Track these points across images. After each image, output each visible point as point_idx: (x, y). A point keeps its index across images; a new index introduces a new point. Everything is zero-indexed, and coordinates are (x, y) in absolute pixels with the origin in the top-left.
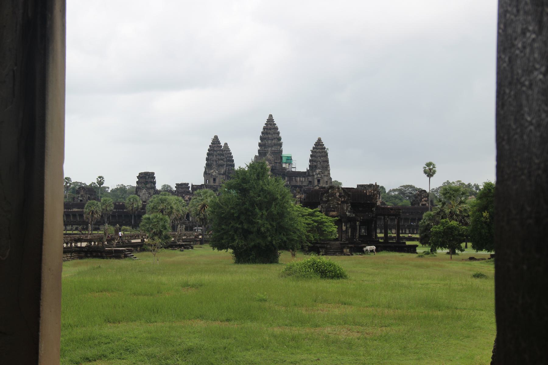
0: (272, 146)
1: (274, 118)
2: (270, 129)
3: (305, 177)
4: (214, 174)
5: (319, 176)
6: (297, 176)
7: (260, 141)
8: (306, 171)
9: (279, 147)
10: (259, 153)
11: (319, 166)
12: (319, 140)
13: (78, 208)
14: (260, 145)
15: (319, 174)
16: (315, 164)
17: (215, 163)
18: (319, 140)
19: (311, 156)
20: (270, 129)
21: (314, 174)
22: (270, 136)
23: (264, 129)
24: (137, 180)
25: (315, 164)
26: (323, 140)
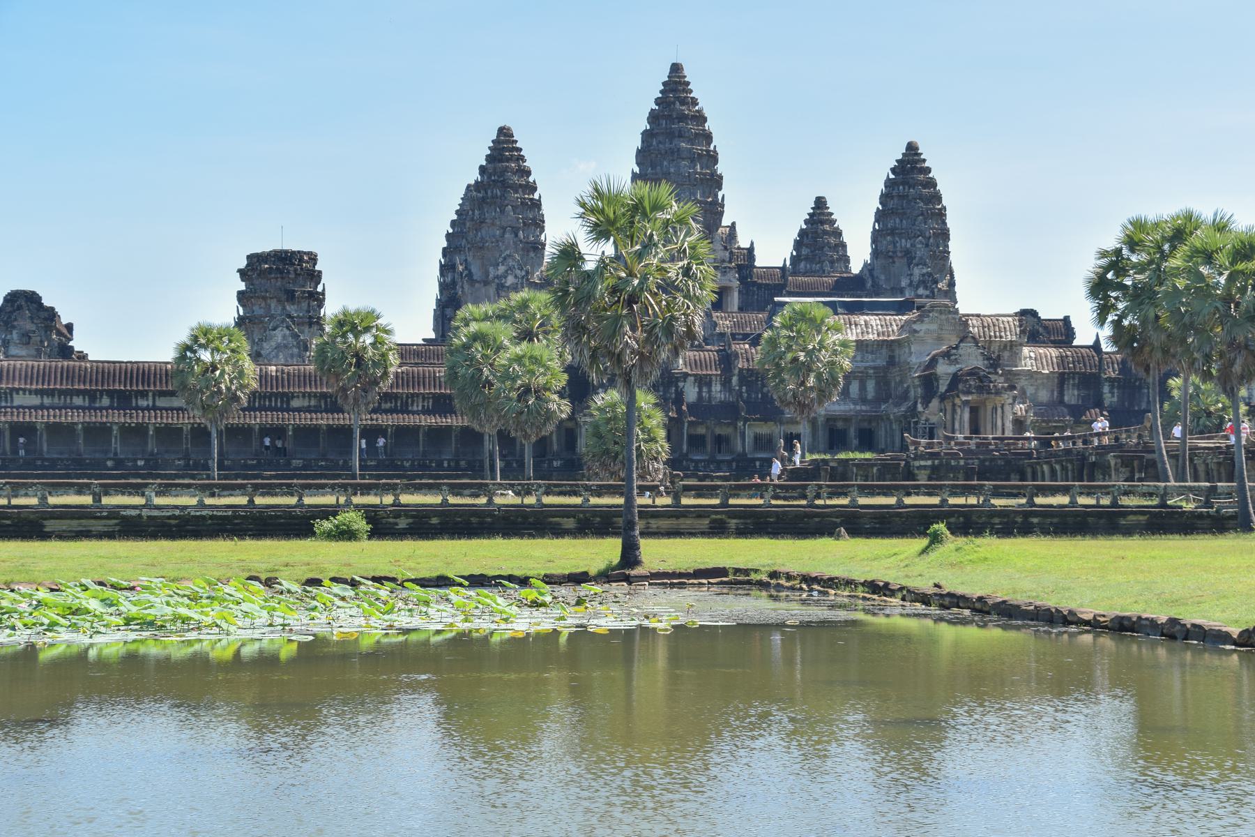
2: (683, 118)
4: (510, 280)
5: (921, 291)
12: (912, 148)
16: (905, 243)
18: (912, 148)
23: (653, 117)
24: (242, 286)
25: (905, 243)
26: (925, 151)
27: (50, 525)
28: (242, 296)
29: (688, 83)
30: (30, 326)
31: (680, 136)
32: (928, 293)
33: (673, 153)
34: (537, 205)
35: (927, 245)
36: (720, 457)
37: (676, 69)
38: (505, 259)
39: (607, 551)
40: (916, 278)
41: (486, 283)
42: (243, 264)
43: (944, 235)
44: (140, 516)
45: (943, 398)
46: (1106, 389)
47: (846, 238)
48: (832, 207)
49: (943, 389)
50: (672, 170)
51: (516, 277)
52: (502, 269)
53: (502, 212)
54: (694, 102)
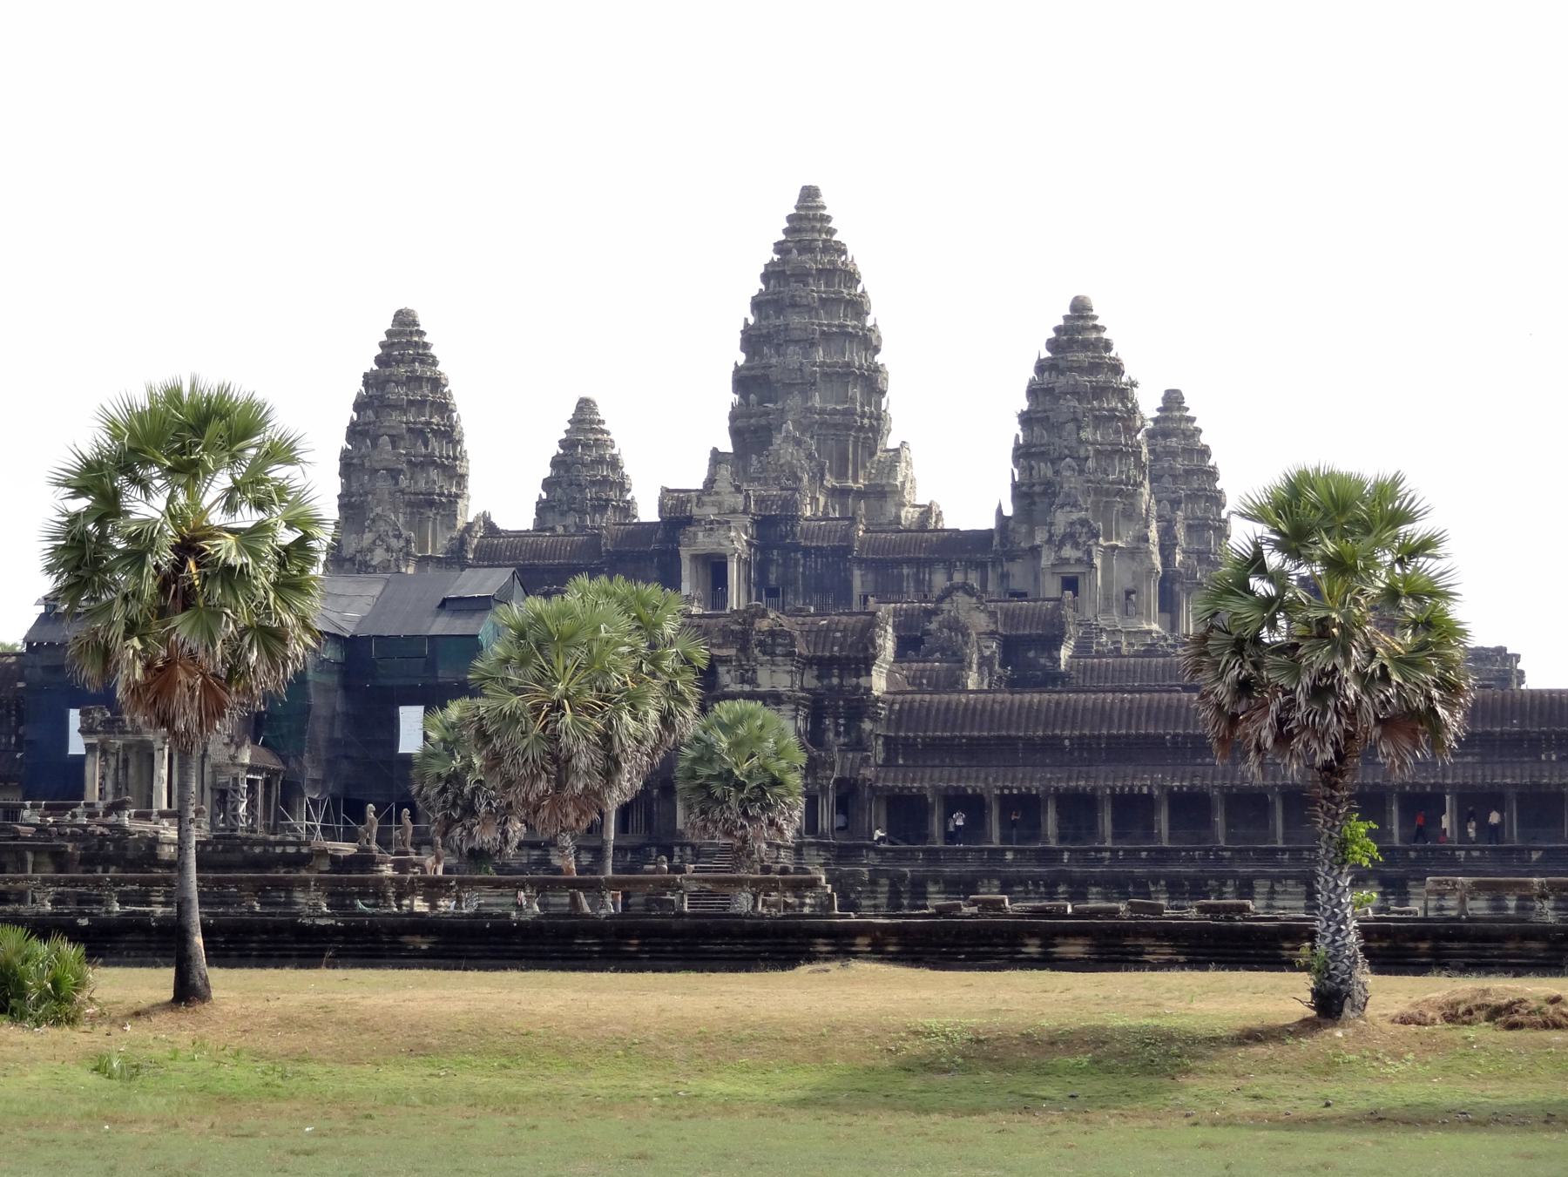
0: (808, 386)
1: (831, 203)
3: (981, 566)
6: (929, 563)
7: (741, 358)
8: (989, 523)
9: (856, 392)
10: (736, 433)
11: (1071, 481)
14: (743, 381)
15: (1070, 537)
16: (1046, 470)
17: (383, 485)
18: (1080, 310)
19: (1026, 419)
21: (1040, 537)
22: (796, 320)
25: (1046, 470)
26: (1105, 314)
29: (828, 219)
31: (794, 305)
32: (1079, 554)
33: (778, 332)
35: (1081, 472)
37: (809, 195)
38: (373, 521)
40: (1060, 528)
50: (774, 361)
51: (388, 549)
52: (368, 537)
53: (375, 445)
54: (840, 250)
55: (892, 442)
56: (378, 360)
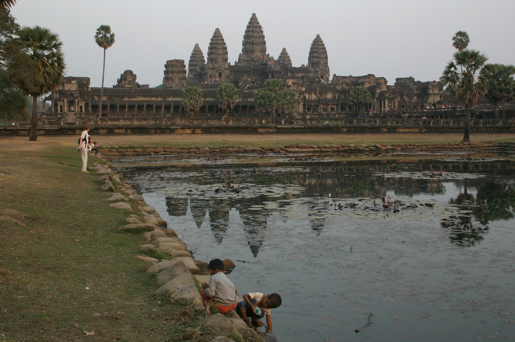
13: (145, 96)
18: (318, 36)
20: (256, 27)
21: (318, 69)
23: (248, 27)
25: (317, 60)
27: (260, 130)
28: (166, 72)
30: (130, 80)
34: (226, 48)
36: (315, 113)
37: (254, 16)
39: (459, 138)
41: (215, 69)
42: (166, 64)
43: (327, 58)
44: (281, 128)
45: (378, 99)
46: (405, 97)
47: (291, 58)
48: (287, 50)
49: (377, 96)
55: (267, 54)
56: (213, 37)
